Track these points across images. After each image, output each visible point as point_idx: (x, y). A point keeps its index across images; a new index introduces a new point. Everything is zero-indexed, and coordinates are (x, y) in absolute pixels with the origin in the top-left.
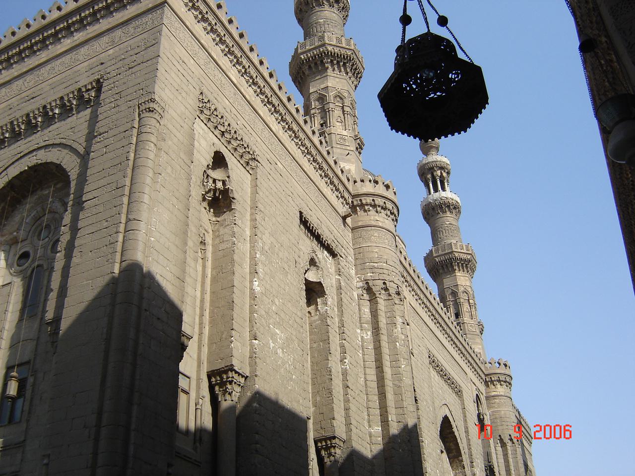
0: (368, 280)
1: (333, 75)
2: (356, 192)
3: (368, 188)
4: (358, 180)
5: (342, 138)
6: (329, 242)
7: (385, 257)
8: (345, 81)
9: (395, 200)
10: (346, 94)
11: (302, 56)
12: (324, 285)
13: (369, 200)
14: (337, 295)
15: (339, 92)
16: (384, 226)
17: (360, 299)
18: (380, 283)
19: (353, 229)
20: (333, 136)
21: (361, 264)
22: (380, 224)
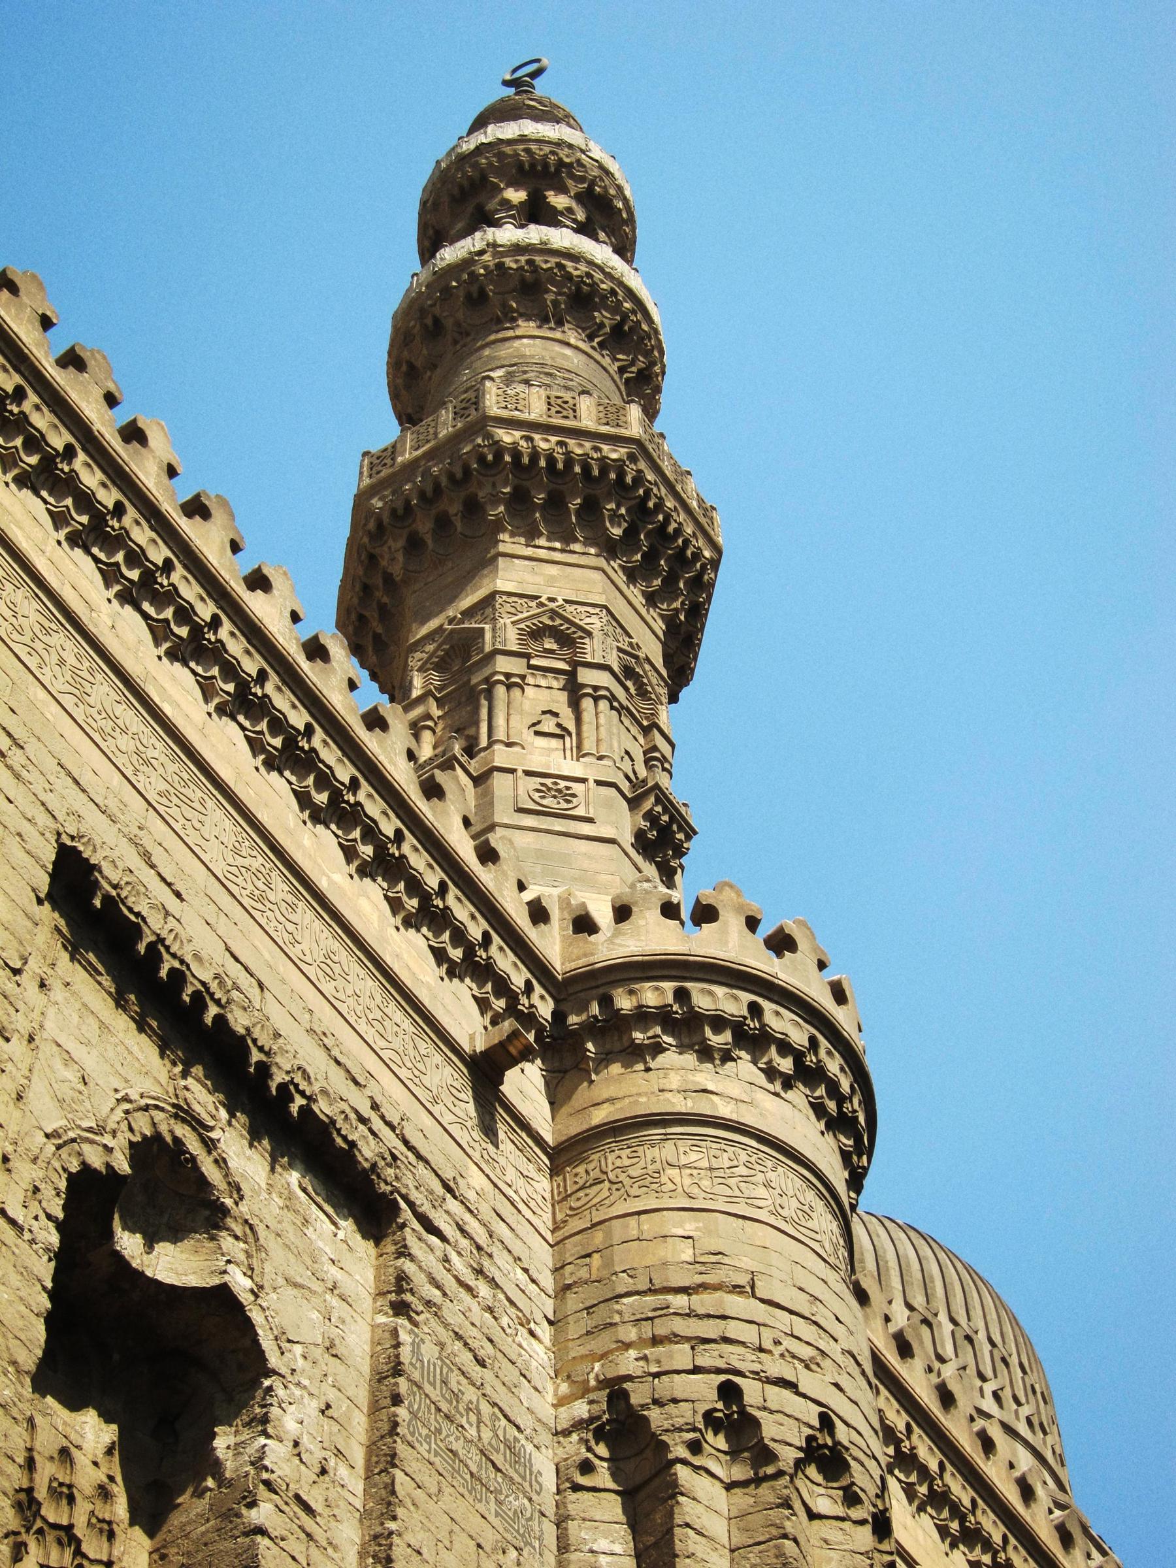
0: (629, 1378)
1: (529, 552)
2: (581, 962)
3: (654, 937)
4: (602, 914)
5: (556, 787)
6: (323, 1108)
7: (747, 1263)
8: (597, 576)
9: (841, 1015)
10: (595, 623)
11: (373, 501)
12: (256, 1316)
13: (655, 994)
14: (375, 1408)
15: (554, 614)
16: (749, 1118)
17: (569, 1486)
18: (704, 1390)
19: (562, 1156)
20: (500, 783)
21: (587, 1291)
22: (725, 1110)
